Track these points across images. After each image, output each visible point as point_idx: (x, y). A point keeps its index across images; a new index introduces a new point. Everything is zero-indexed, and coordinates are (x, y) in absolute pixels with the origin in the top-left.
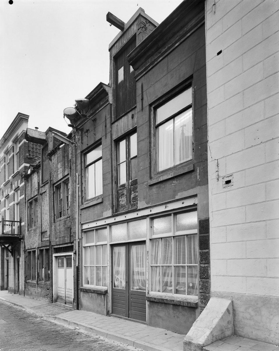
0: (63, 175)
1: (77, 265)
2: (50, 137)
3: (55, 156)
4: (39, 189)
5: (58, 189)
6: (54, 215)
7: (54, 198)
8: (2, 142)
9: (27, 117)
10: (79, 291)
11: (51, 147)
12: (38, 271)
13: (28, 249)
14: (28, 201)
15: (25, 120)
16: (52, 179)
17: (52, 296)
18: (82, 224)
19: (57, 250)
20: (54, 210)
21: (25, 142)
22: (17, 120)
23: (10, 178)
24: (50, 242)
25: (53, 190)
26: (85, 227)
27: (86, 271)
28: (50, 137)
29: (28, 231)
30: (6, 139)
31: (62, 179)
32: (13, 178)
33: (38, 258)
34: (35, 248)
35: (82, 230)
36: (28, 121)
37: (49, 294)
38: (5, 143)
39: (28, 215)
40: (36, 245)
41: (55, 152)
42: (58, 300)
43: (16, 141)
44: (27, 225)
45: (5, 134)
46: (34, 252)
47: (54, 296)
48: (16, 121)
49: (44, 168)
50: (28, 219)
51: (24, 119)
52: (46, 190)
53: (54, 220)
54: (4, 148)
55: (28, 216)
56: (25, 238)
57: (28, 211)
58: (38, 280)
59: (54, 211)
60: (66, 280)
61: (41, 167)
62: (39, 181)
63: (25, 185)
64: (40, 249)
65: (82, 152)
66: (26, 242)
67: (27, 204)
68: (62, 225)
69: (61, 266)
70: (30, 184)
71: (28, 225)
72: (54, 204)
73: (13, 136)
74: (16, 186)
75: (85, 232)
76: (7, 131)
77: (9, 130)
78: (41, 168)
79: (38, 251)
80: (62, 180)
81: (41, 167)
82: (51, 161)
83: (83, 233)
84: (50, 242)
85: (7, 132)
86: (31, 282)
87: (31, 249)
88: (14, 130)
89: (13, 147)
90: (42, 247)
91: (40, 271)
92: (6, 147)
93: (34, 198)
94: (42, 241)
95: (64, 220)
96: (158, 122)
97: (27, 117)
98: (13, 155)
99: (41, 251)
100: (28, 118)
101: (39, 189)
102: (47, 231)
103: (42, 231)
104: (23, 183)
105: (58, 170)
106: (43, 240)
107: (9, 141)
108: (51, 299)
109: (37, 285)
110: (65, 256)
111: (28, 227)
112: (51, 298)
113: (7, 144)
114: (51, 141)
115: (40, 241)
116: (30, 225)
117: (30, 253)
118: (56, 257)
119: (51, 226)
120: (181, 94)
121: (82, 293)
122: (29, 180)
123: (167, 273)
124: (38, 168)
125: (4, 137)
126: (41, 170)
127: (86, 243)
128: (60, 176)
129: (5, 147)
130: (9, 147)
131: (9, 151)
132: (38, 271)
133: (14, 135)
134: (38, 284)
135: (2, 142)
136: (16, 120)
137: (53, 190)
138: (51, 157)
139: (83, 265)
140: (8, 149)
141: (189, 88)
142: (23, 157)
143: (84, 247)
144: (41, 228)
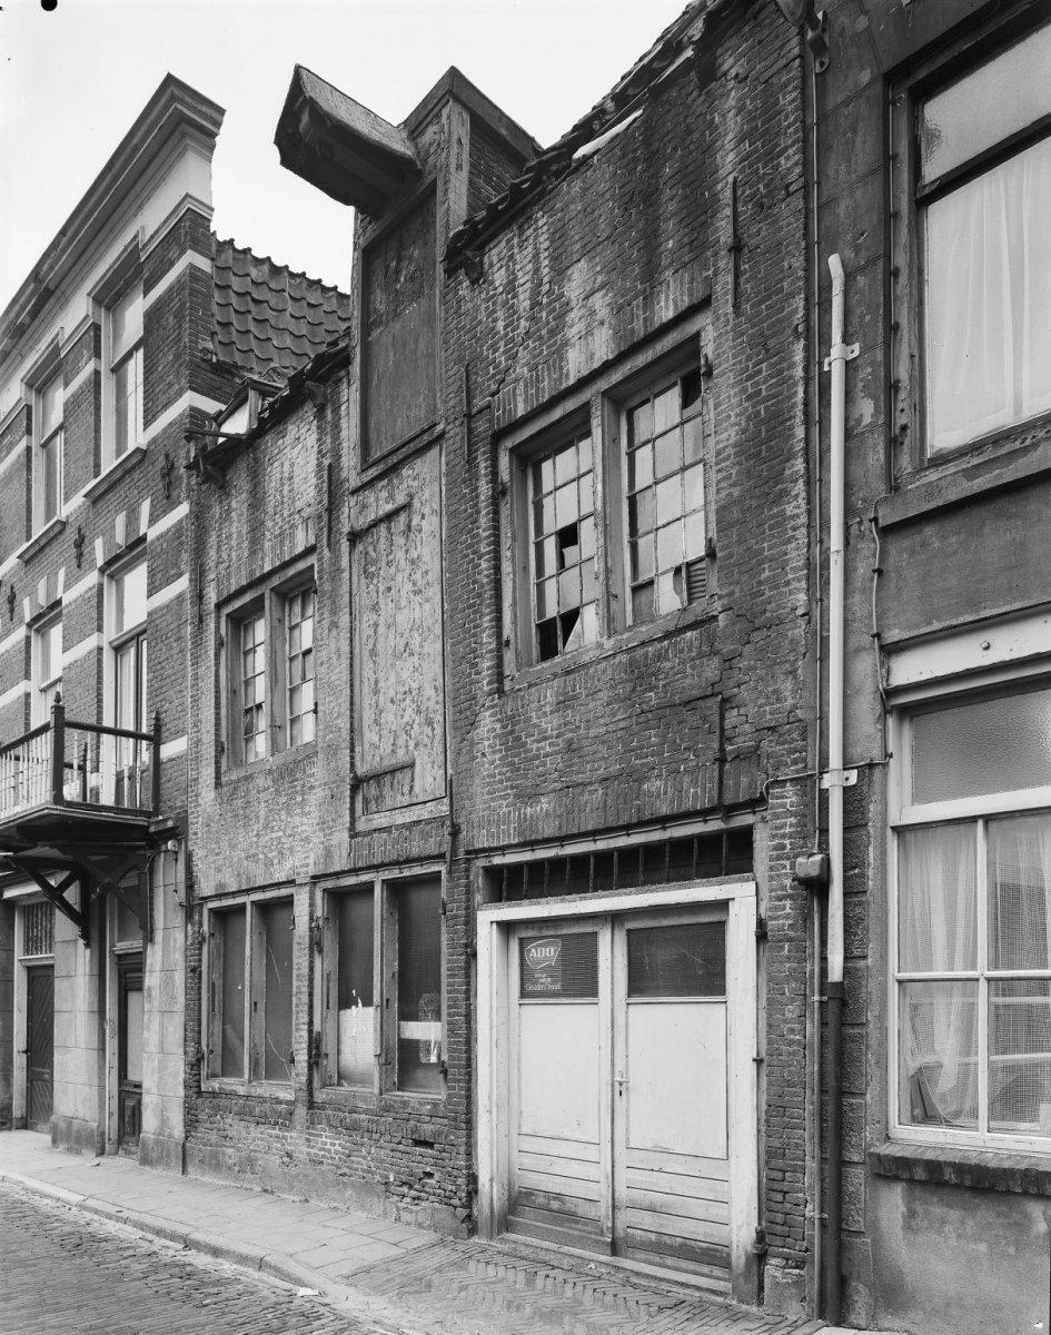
0: (617, 335)
1: (836, 974)
2: (455, 137)
3: (520, 236)
4: (332, 508)
5: (524, 472)
6: (502, 645)
7: (496, 528)
8: (18, 316)
9: (215, 115)
10: (857, 1178)
11: (455, 204)
12: (311, 1023)
13: (219, 896)
14: (219, 606)
15: (197, 134)
16: (479, 402)
17: (473, 1193)
18: (890, 650)
19: (507, 883)
20: (499, 610)
21: (192, 267)
22: (143, 140)
23: (78, 500)
24: (455, 833)
25: (494, 473)
26: (911, 669)
27: (917, 1014)
28: (455, 137)
29: (218, 784)
30: (43, 292)
31: (607, 367)
32: (95, 502)
33: (316, 945)
34: (291, 882)
35: (891, 693)
36: (212, 148)
37: (430, 1175)
38: (37, 321)
39: (217, 692)
40: (301, 860)
41: (533, 203)
42: (526, 1218)
43: (111, 298)
44: (209, 751)
45: (46, 255)
46: (274, 910)
47: (491, 1192)
48: (136, 149)
49: (385, 360)
50: (218, 715)
51: (191, 130)
52: (411, 496)
53: (499, 677)
54: (23, 357)
55: (217, 698)
56: (196, 826)
57: (217, 664)
58: (310, 1082)
59: (498, 620)
60: (619, 1088)
61: (357, 361)
62: (337, 456)
63: (199, 517)
64: (330, 884)
65: (891, 78)
66: (198, 854)
67: (212, 626)
68: (604, 695)
69: (558, 987)
70: (239, 502)
71: (220, 750)
72: (497, 569)
73: (98, 261)
74: (120, 537)
75: (907, 713)
76: (63, 232)
77: (109, 178)
78: (356, 368)
79: (312, 898)
80: (603, 385)
81: (357, 361)
82: (474, 282)
83: (891, 722)
84: (455, 833)
85: (65, 240)
86: (242, 1091)
87: (248, 891)
88: (115, 217)
89: (96, 327)
90: (355, 871)
91: (331, 1024)
92: (48, 338)
93: (276, 581)
94: (354, 834)
95: (624, 658)
96: (934, 169)
97: (215, 115)
98: (97, 373)
99: (340, 900)
100: (218, 124)
101: (332, 508)
102: (412, 765)
103: (361, 770)
104: (183, 510)
105: (561, 316)
106: (361, 826)
107: (64, 302)
108: (462, 1212)
109: (301, 1112)
110: (615, 918)
111: (218, 763)
112: (455, 1202)
113: (50, 325)
114: (459, 167)
115: (342, 836)
116: (234, 752)
117: (226, 918)
118: (507, 928)
119: (463, 717)
120: (968, 74)
121: (893, 1201)
122: (240, 480)
123: (816, 991)
124: (332, 371)
125: (35, 276)
126: (356, 386)
127: (920, 796)
128: (859, 193)
129: (31, 348)
130: (66, 336)
131: (60, 364)
132: (311, 1023)
133: (114, 240)
134: (311, 1105)
135: (18, 316)
136: (135, 141)
137: (494, 473)
138: (482, 256)
139: (894, 972)
140: (56, 350)
141: (1032, 33)
142: (177, 357)
143: (899, 831)
144: (352, 750)
